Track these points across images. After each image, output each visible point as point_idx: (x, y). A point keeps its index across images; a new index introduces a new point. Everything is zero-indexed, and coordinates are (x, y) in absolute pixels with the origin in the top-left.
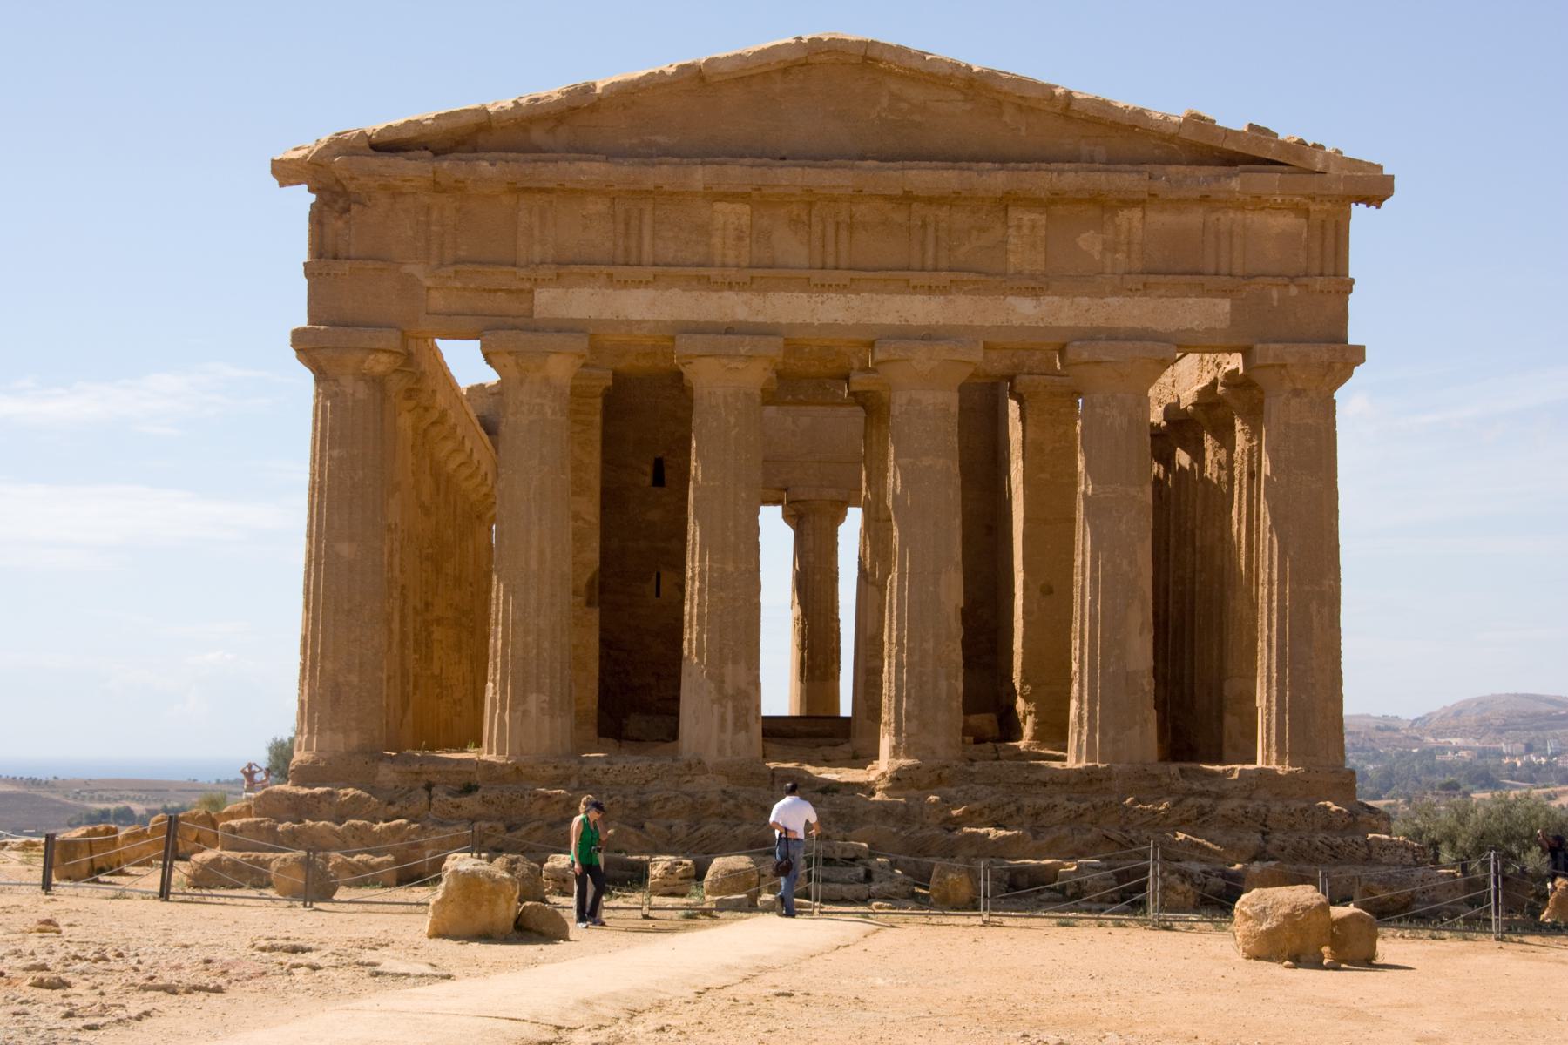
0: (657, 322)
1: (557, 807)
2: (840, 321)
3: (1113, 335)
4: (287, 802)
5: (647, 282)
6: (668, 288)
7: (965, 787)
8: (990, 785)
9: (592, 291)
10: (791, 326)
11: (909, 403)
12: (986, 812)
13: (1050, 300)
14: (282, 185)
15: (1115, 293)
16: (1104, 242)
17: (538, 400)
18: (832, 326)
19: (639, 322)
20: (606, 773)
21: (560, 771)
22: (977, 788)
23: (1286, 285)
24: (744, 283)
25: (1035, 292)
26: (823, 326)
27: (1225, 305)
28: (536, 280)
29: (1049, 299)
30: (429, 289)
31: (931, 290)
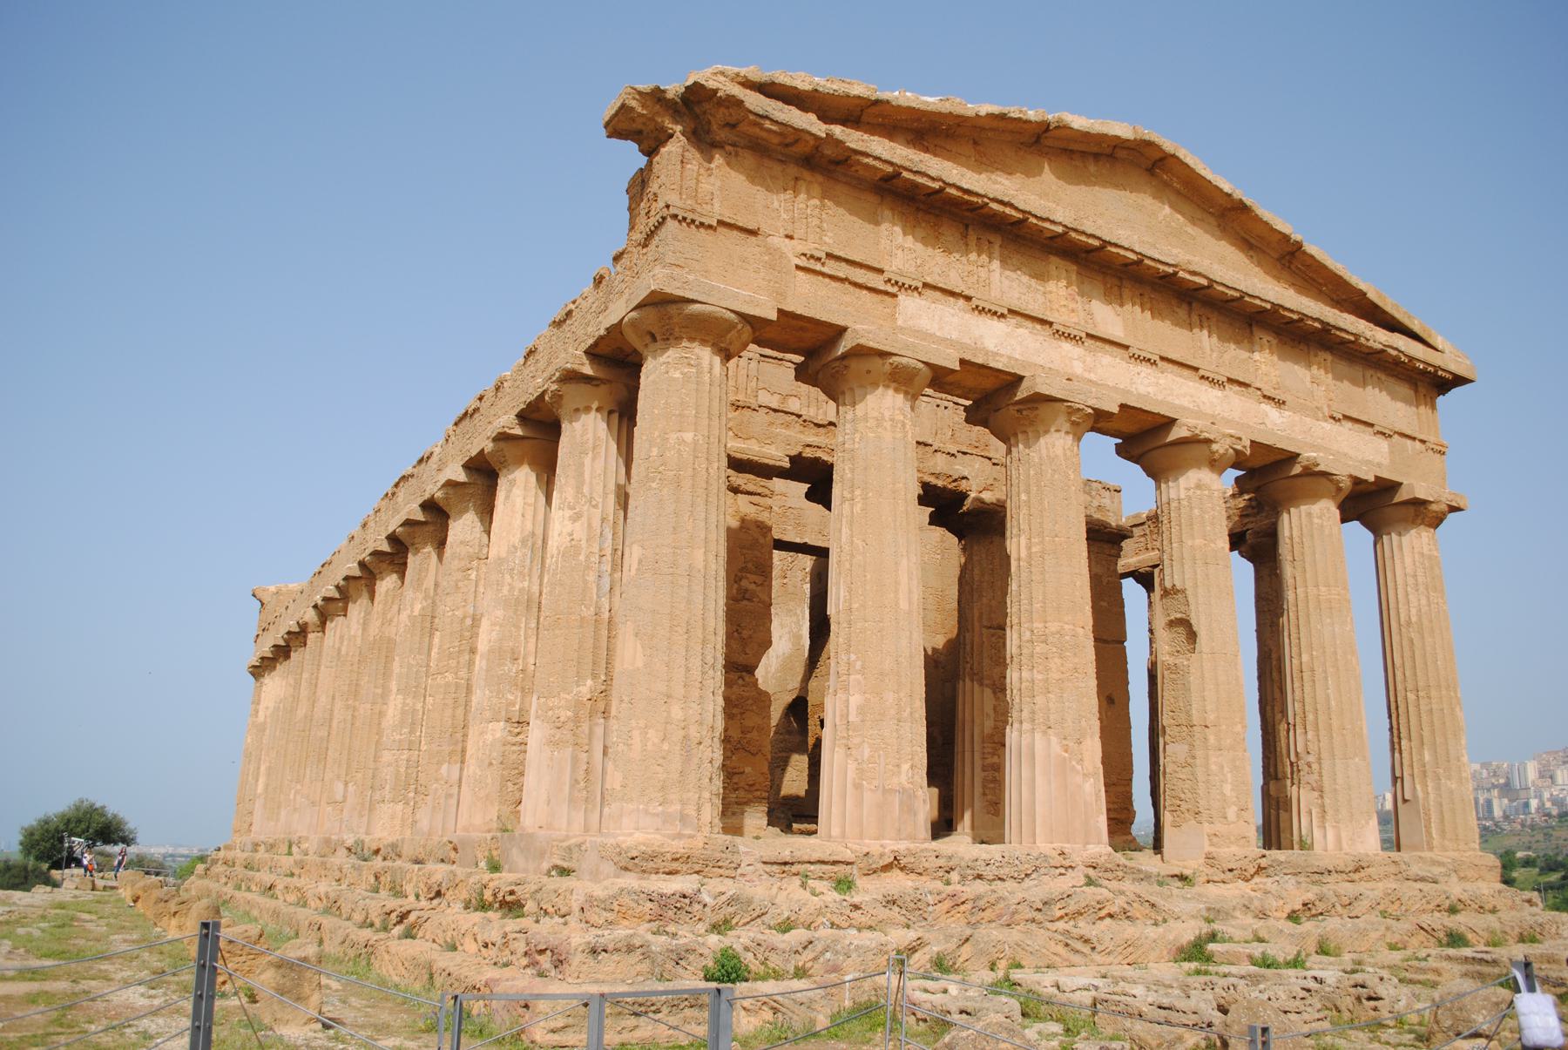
0: (1010, 358)
1: (962, 908)
4: (649, 905)
5: (1002, 316)
6: (1018, 326)
7: (1277, 878)
8: (1295, 874)
9: (952, 311)
11: (1198, 487)
17: (902, 418)
18: (1146, 397)
20: (988, 865)
21: (941, 862)
22: (1287, 877)
23: (1414, 439)
24: (1081, 338)
25: (1280, 403)
26: (1140, 396)
27: (1383, 444)
28: (904, 284)
30: (798, 267)
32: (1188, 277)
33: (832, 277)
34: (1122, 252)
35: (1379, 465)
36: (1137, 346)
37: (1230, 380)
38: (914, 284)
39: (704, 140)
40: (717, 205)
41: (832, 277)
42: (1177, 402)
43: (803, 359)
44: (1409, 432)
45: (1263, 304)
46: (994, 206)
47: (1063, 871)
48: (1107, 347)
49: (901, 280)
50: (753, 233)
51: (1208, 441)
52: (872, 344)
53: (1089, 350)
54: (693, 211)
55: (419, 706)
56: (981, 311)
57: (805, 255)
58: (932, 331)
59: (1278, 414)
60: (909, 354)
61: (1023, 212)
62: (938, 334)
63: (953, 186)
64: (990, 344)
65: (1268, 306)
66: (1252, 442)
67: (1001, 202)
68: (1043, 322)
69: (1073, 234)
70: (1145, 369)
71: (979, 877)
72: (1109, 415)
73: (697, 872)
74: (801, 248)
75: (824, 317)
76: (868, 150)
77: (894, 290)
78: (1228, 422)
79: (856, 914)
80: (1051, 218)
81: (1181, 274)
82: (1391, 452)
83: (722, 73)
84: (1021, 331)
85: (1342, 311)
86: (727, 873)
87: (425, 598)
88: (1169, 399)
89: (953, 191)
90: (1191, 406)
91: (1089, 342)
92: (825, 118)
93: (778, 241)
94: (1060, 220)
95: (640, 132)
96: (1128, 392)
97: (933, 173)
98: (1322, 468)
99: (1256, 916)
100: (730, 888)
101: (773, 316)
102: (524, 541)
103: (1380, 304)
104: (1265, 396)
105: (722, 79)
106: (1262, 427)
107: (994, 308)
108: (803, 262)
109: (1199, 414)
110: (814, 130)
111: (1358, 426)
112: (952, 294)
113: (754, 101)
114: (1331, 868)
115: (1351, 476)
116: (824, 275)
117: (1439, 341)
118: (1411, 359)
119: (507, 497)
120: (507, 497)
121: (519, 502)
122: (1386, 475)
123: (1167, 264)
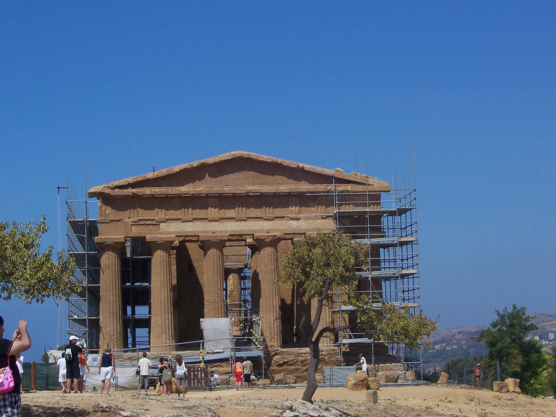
2: (244, 229)
5: (191, 221)
6: (197, 222)
10: (231, 231)
12: (289, 362)
13: (300, 222)
15: (318, 219)
29: (301, 221)
30: (132, 225)
31: (268, 220)
32: (252, 194)
38: (164, 220)
49: (160, 220)
50: (119, 220)
54: (104, 220)
59: (297, 222)
63: (170, 194)
68: (205, 219)
70: (243, 223)
77: (159, 223)
80: (201, 193)
81: (250, 194)
90: (260, 229)
94: (204, 193)
104: (290, 219)
105: (105, 188)
106: (289, 228)
107: (188, 220)
108: (132, 224)
109: (262, 231)
116: (139, 225)
117: (371, 181)
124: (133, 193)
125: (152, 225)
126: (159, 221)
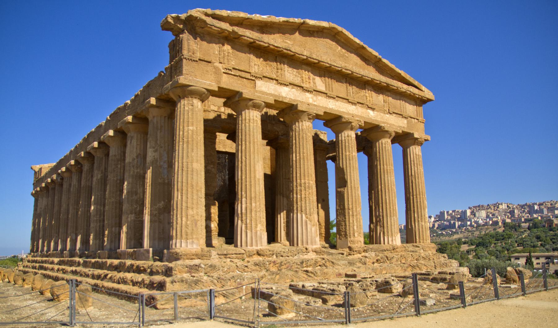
0: (290, 99)
3: (388, 124)
5: (288, 85)
6: (292, 88)
11: (348, 136)
14: (163, 30)
16: (384, 100)
18: (332, 109)
19: (286, 98)
21: (271, 252)
25: (373, 109)
26: (330, 109)
27: (405, 121)
30: (224, 73)
31: (353, 104)
32: (346, 71)
33: (234, 75)
34: (325, 64)
35: (404, 127)
36: (329, 93)
37: (358, 103)
38: (260, 76)
39: (195, 34)
40: (198, 54)
41: (234, 75)
42: (342, 110)
43: (226, 100)
44: (413, 117)
45: (369, 79)
46: (285, 51)
47: (306, 253)
48: (320, 94)
49: (256, 75)
50: (210, 62)
51: (351, 123)
52: (247, 97)
53: (314, 95)
54: (191, 56)
55: (102, 208)
56: (281, 84)
57: (226, 69)
58: (266, 91)
60: (259, 99)
61: (294, 52)
62: (268, 92)
64: (284, 95)
65: (370, 79)
66: (365, 122)
67: (287, 50)
69: (309, 59)
70: (331, 100)
71: (282, 256)
72: (320, 115)
73: (199, 259)
74: (224, 66)
75: (232, 88)
76: (245, 35)
77: (254, 78)
78: (357, 116)
79: (246, 269)
82: (408, 123)
83: (199, 11)
84: (294, 90)
85: (393, 80)
86: (208, 258)
87: (102, 173)
88: (339, 109)
89: (271, 47)
91: (314, 92)
92: (231, 25)
93: (217, 64)
95: (172, 29)
96: (327, 108)
97: (266, 41)
98: (386, 129)
99: (363, 264)
100: (209, 262)
101: (217, 89)
102: (137, 157)
103: (405, 77)
104: (369, 107)
105: (199, 13)
107: (285, 83)
110: (228, 29)
111: (397, 115)
112: (272, 79)
113: (209, 20)
114: (386, 249)
115: (395, 131)
117: (423, 88)
118: (414, 94)
119: (131, 143)
120: (131, 143)
121: (135, 144)
122: (406, 130)
123: (339, 67)
124: (233, 31)
125: (246, 78)
126: (255, 76)
